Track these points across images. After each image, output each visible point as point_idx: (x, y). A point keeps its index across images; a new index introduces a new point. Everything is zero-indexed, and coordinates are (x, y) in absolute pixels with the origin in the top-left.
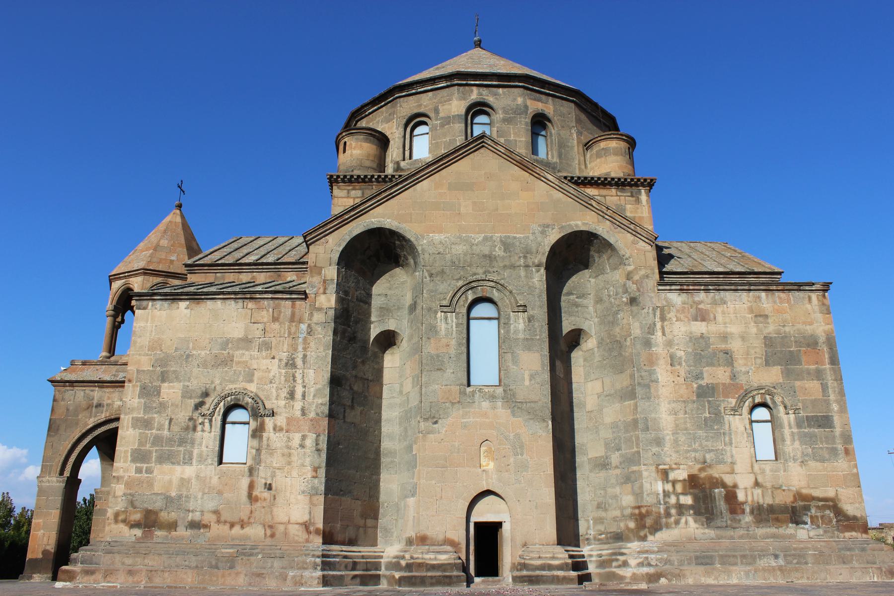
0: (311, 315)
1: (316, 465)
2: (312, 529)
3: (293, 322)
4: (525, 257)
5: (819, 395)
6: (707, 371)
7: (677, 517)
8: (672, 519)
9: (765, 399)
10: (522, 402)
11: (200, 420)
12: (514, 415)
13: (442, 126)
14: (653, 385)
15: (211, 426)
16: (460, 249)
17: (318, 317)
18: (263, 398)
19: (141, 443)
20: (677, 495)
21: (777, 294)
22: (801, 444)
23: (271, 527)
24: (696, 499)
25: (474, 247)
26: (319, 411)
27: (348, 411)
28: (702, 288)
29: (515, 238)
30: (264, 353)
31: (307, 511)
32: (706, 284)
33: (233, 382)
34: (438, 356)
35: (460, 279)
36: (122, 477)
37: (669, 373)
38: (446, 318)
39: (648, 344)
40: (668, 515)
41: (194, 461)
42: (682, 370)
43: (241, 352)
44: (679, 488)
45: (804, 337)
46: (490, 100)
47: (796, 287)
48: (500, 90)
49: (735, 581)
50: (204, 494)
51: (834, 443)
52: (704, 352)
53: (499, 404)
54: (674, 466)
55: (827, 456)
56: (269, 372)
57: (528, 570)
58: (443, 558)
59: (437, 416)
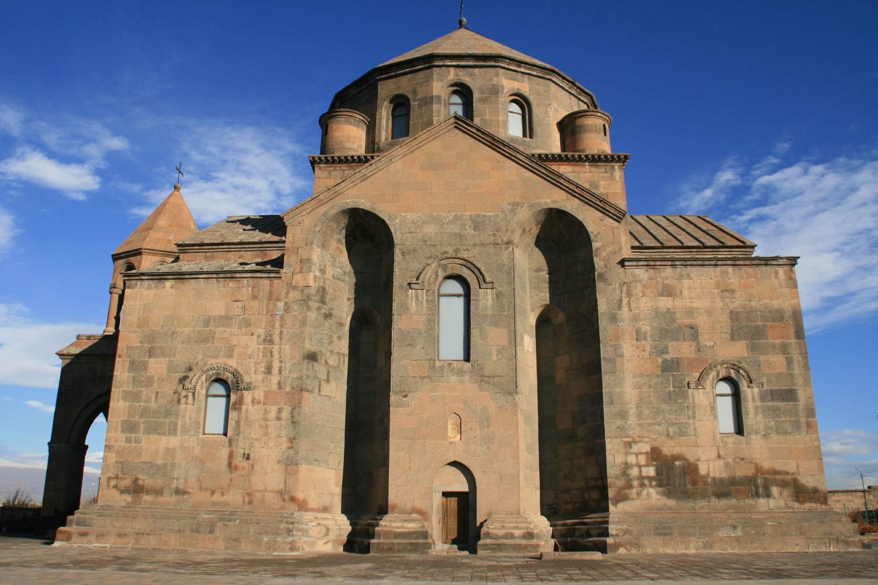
0: (287, 293)
1: (291, 436)
2: (287, 497)
3: (271, 300)
4: (494, 235)
5: (785, 371)
6: (672, 345)
7: (639, 489)
8: (634, 491)
9: (730, 373)
10: (489, 377)
11: (184, 393)
12: (481, 389)
13: (420, 106)
14: (619, 360)
15: (194, 399)
16: (431, 230)
17: (294, 295)
18: (242, 372)
19: (130, 415)
20: (640, 466)
21: (744, 268)
22: (764, 416)
23: (249, 494)
24: (658, 472)
25: (445, 226)
26: (295, 385)
27: (323, 384)
28: (669, 263)
29: (485, 216)
30: (244, 330)
31: (282, 480)
32: (673, 260)
33: (216, 357)
34: (409, 332)
35: (431, 257)
36: (114, 446)
37: (634, 348)
38: (417, 296)
39: (614, 319)
40: (630, 487)
41: (178, 433)
42: (648, 345)
43: (222, 329)
44: (642, 460)
45: (770, 312)
46: (467, 80)
47: (763, 262)
48: (477, 71)
49: (692, 551)
50: (187, 463)
51: (797, 415)
52: (669, 328)
53: (467, 378)
54: (637, 439)
55: (789, 429)
56: (248, 348)
57: (491, 538)
58: (412, 526)
59: (407, 390)
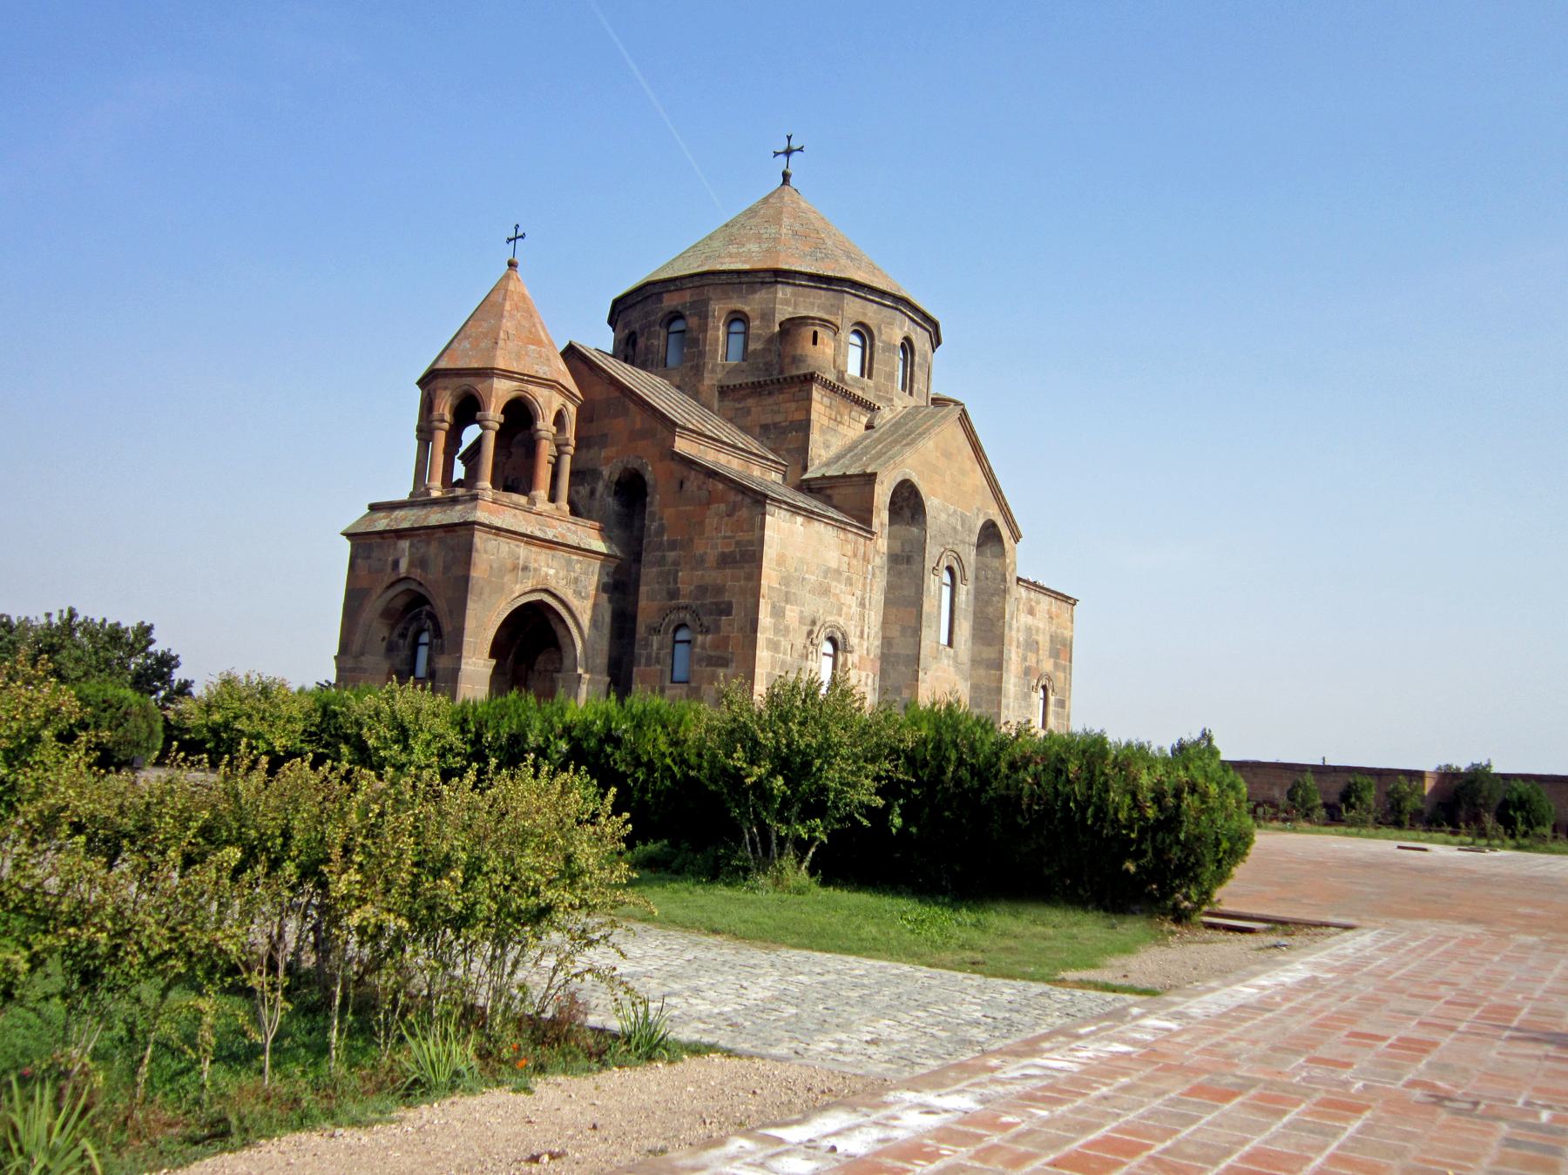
13: (884, 351)
19: (773, 668)
33: (831, 613)
46: (914, 338)
